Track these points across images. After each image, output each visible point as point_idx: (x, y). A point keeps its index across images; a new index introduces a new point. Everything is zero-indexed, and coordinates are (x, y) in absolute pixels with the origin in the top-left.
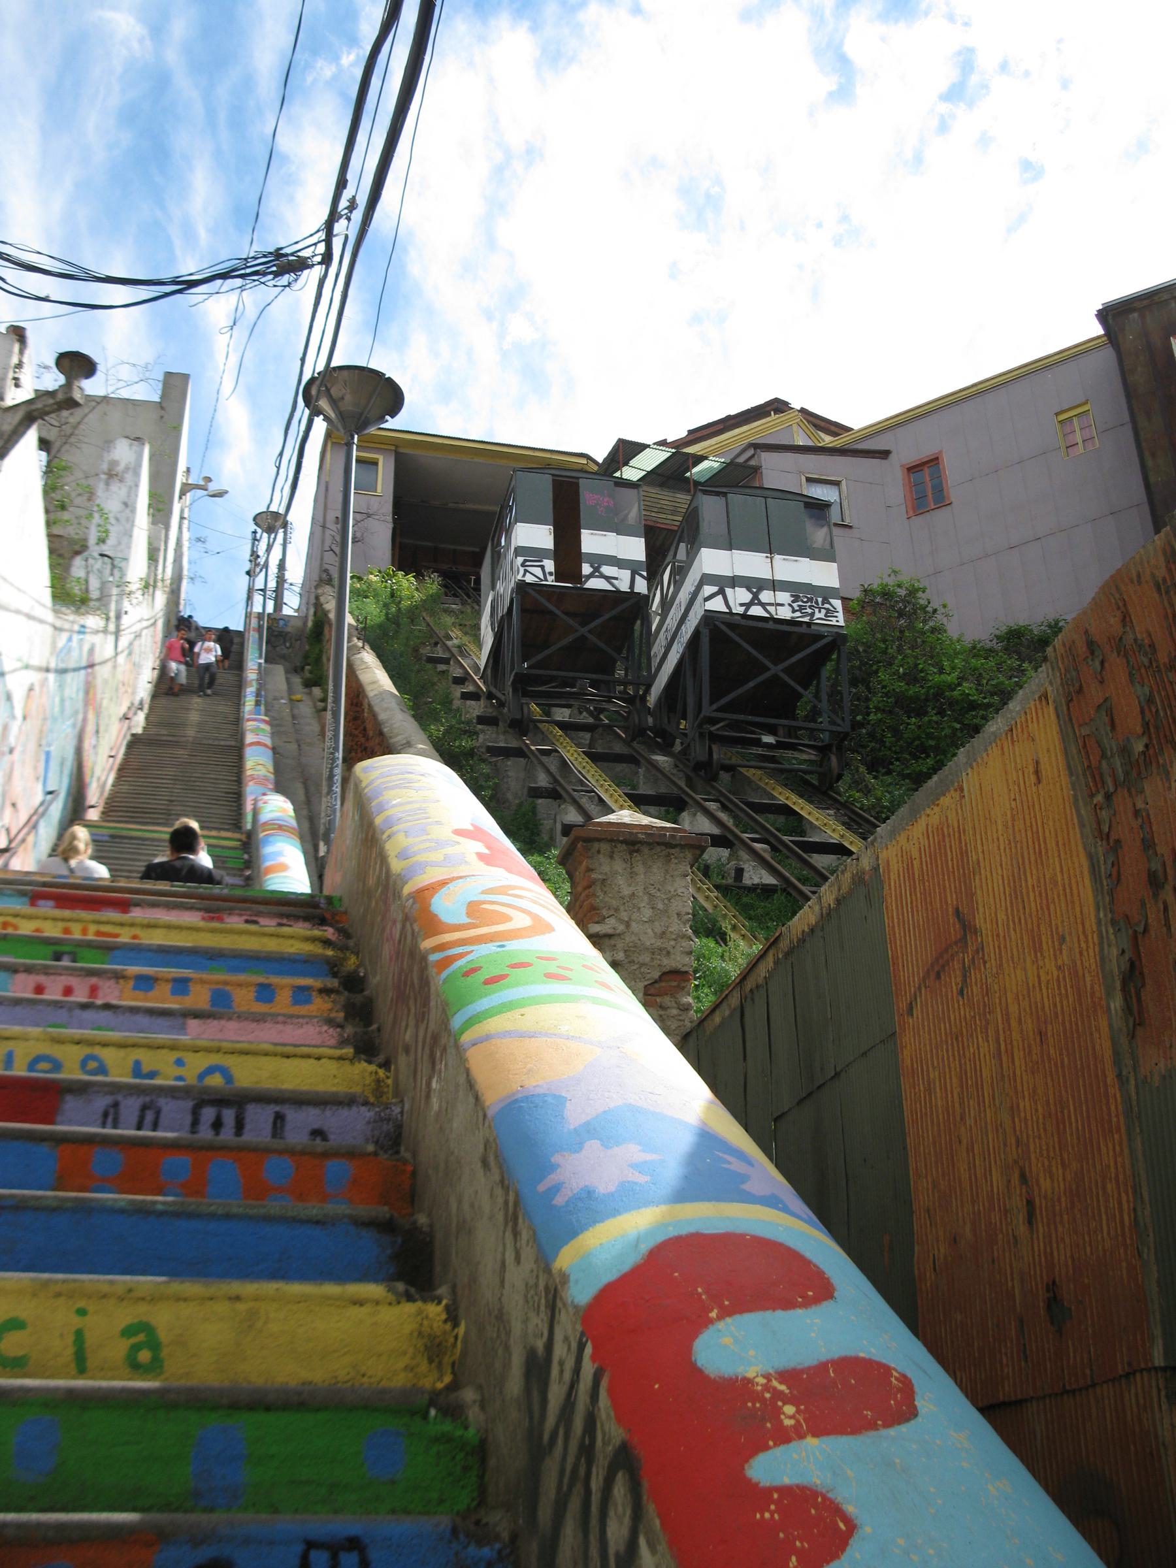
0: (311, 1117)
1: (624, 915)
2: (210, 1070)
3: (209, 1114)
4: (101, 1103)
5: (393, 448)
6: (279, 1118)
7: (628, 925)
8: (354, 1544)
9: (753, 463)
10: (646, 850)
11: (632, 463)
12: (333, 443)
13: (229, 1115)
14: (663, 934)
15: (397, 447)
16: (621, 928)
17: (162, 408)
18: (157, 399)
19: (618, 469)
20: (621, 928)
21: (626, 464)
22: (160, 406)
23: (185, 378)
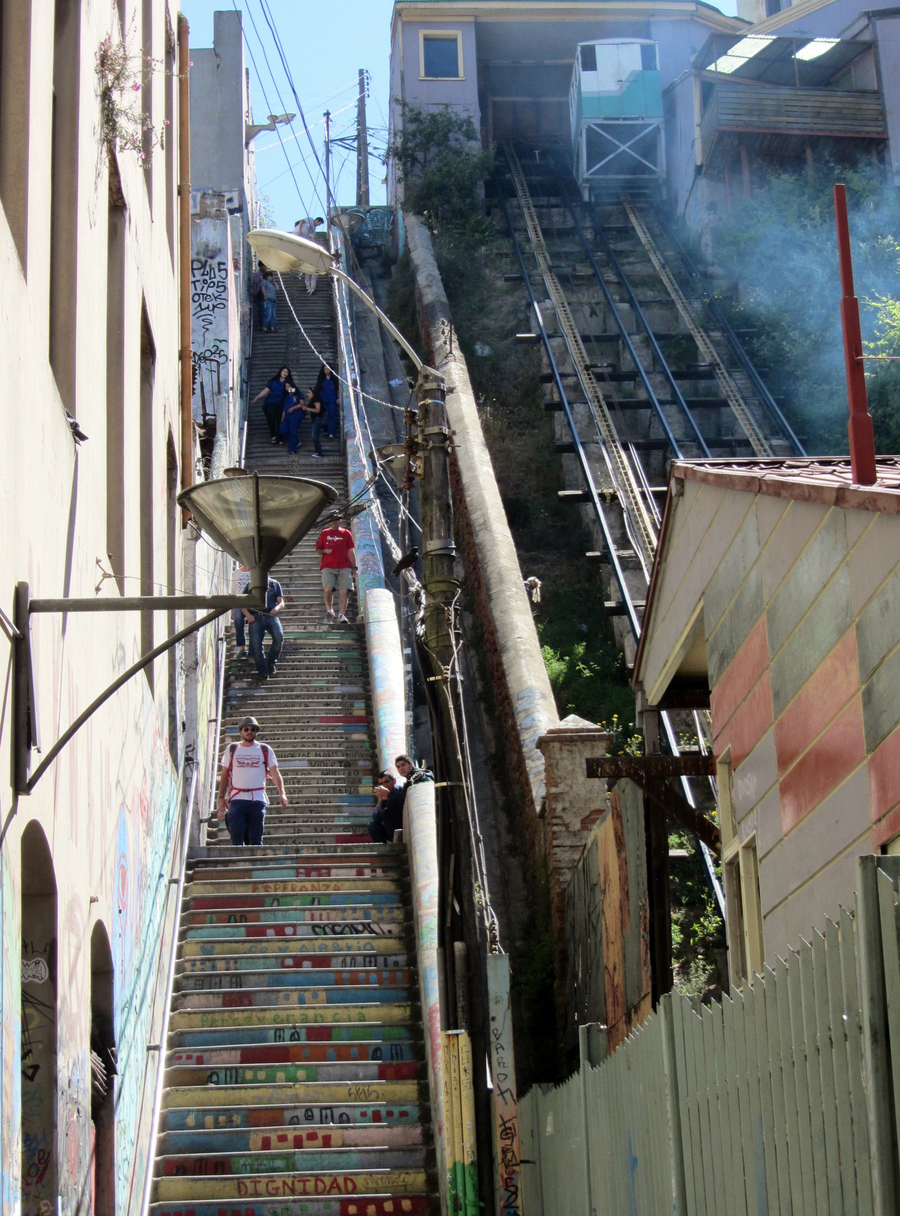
0: (394, 958)
1: (569, 782)
2: (367, 944)
3: (368, 959)
4: (341, 959)
5: (472, 19)
6: (385, 960)
7: (571, 787)
8: (399, 1045)
9: (866, 37)
10: (579, 743)
11: (730, 52)
12: (404, 23)
13: (373, 959)
14: (590, 791)
15: (476, 17)
16: (567, 789)
17: (217, 55)
18: (212, 46)
19: (714, 61)
20: (567, 789)
21: (725, 53)
22: (214, 53)
23: (238, 14)
